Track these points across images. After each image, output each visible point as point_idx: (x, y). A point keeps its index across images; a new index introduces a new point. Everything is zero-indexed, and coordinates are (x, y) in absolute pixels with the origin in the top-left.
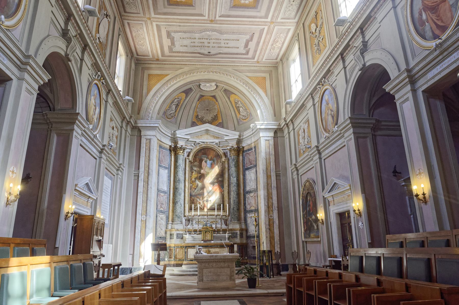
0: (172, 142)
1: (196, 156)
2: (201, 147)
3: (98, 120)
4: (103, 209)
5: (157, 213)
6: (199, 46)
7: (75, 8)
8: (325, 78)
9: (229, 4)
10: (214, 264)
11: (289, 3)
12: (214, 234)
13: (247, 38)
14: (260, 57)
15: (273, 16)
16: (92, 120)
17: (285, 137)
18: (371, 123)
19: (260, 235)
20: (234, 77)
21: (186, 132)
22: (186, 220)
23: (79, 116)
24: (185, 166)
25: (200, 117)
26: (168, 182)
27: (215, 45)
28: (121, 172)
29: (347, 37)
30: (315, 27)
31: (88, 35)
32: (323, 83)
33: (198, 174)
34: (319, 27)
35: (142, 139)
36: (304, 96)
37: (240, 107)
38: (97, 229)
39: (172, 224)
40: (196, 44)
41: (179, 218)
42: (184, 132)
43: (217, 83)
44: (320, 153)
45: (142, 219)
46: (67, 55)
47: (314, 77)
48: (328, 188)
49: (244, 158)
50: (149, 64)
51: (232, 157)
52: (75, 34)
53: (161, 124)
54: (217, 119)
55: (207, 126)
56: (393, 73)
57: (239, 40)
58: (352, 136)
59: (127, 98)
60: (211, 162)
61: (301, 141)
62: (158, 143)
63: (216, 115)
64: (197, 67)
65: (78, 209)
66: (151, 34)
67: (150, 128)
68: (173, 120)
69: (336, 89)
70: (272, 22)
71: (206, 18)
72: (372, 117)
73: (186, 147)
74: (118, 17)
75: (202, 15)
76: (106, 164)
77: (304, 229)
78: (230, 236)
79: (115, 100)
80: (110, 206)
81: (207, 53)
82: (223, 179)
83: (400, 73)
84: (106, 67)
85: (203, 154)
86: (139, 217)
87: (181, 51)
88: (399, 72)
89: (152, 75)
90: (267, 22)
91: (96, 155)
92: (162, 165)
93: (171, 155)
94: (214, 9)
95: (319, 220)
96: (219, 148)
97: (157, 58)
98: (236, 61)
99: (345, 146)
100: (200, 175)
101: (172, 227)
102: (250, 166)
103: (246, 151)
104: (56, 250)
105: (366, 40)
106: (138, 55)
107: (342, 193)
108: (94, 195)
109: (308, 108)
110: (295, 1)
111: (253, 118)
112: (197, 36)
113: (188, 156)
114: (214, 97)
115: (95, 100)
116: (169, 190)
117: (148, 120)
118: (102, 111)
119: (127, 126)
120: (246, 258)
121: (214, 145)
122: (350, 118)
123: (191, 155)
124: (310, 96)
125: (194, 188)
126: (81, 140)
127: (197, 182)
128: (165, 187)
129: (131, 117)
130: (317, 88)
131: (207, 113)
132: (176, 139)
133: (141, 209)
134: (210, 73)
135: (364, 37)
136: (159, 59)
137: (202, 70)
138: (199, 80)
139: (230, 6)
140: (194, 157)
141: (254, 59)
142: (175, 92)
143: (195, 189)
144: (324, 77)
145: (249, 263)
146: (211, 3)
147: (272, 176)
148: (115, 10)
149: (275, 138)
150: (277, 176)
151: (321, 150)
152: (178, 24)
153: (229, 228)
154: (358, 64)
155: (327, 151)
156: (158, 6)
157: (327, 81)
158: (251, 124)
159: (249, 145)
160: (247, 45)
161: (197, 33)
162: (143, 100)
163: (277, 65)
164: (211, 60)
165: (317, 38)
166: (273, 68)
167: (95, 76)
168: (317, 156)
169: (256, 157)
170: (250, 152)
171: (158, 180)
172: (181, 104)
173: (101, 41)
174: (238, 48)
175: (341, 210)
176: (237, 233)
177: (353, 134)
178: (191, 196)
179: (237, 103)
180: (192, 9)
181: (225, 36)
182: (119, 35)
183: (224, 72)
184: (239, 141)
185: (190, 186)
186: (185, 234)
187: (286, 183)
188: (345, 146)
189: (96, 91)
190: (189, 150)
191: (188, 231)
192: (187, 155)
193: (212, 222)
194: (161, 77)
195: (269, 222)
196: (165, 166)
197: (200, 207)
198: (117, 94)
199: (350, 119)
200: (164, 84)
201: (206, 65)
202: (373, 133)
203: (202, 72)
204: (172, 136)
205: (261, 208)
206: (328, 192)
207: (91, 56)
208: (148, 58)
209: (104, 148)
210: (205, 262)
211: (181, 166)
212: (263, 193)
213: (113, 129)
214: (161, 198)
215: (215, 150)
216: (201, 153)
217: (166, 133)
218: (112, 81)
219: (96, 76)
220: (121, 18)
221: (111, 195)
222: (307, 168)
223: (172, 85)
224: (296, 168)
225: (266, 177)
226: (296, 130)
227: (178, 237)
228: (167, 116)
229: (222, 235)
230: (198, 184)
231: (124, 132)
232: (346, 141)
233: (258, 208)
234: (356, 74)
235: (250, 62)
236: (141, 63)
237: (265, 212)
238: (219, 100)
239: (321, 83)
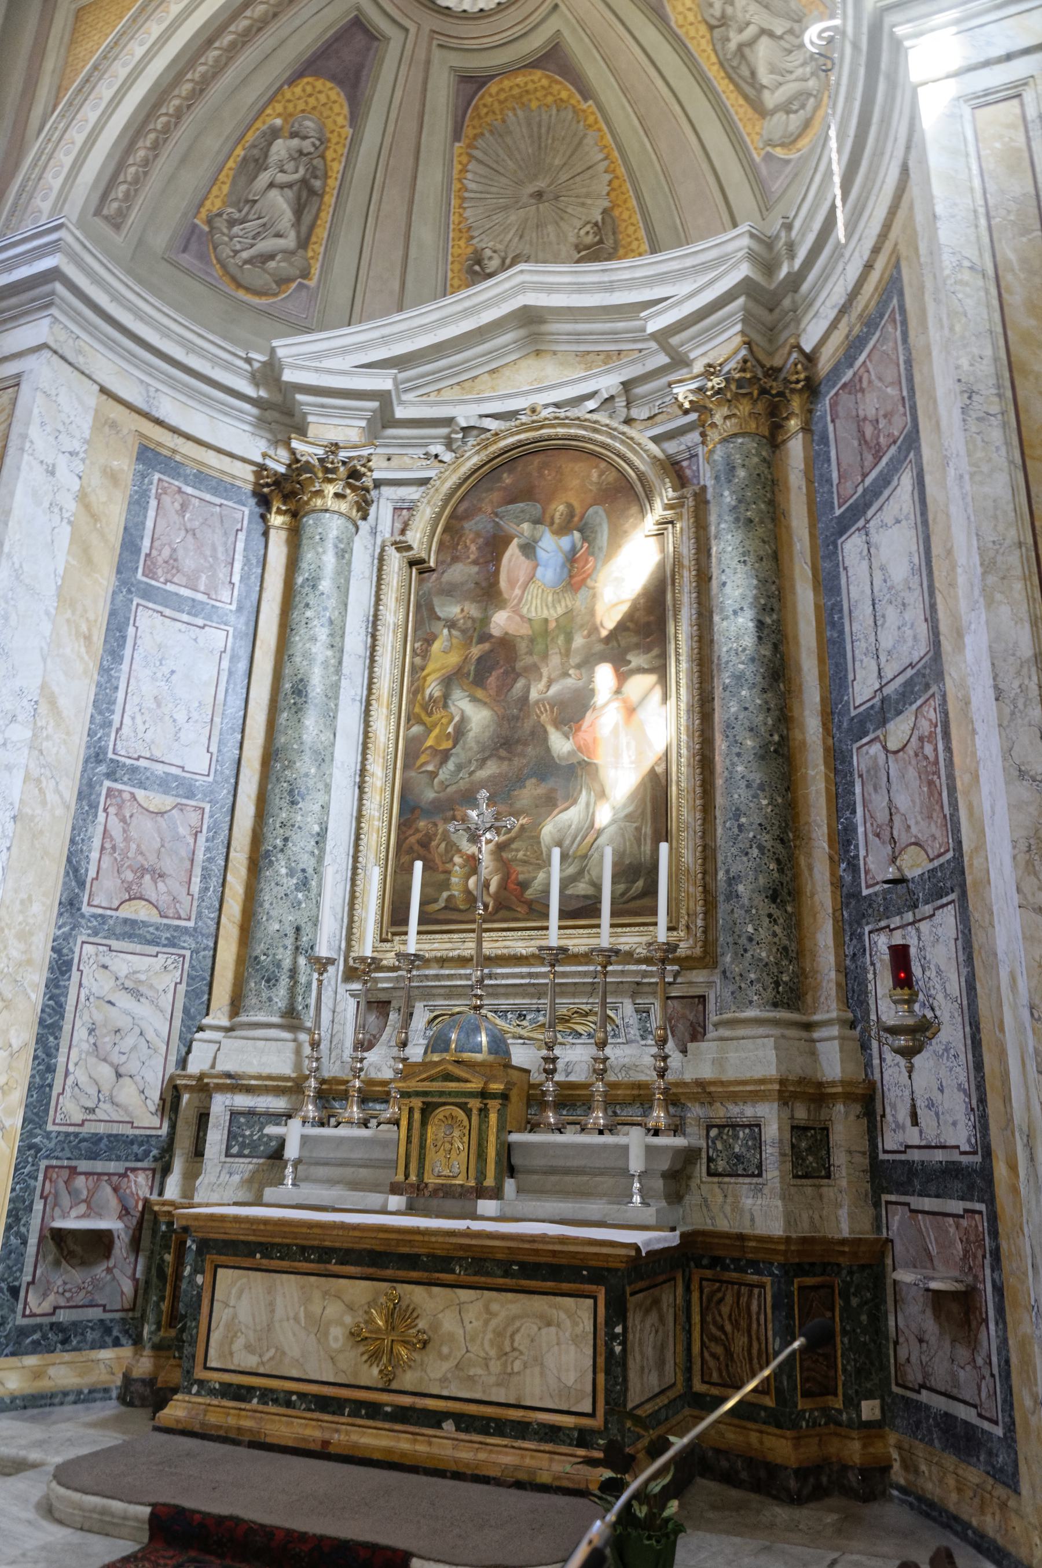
2: (493, 449)
12: (533, 1127)
19: (1000, 1170)
33: (468, 643)
42: (345, 351)
55: (522, 288)
60: (565, 542)
63: (605, 212)
78: (689, 1156)
85: (512, 501)
96: (625, 428)
100: (486, 646)
120: (870, 1409)
125: (434, 751)
127: (462, 704)
131: (540, 226)
140: (445, 530)
143: (445, 756)
172: (333, 183)
176: (755, 1126)
204: (263, 393)
205: (980, 846)
216: (496, 496)
228: (233, 270)
230: (464, 720)
233: (959, 843)
238: (594, 71)
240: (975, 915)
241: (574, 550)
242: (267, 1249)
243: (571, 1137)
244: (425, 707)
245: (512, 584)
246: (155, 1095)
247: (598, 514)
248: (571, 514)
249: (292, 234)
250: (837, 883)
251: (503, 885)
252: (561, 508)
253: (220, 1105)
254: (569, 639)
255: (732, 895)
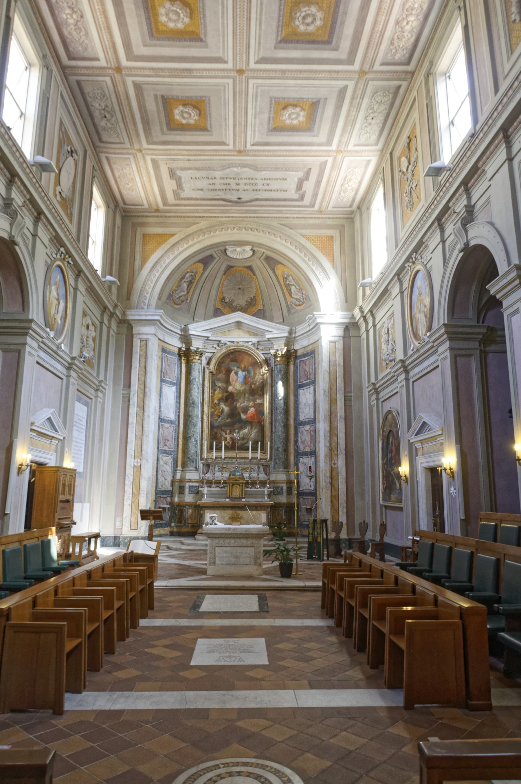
0: (182, 342)
1: (220, 363)
3: (63, 320)
4: (75, 451)
5: (158, 454)
6: (223, 190)
7: (21, 165)
8: (416, 253)
9: (266, 127)
10: (232, 541)
11: (365, 121)
12: (247, 487)
13: (299, 176)
14: (323, 204)
15: (340, 141)
16: (55, 322)
17: (362, 337)
18: (478, 334)
19: (318, 492)
20: (280, 237)
21: (205, 326)
22: (203, 465)
23: (33, 324)
24: (204, 380)
25: (227, 300)
26: (176, 406)
27: (246, 187)
28: (102, 392)
29: (446, 195)
30: (406, 164)
31: (42, 198)
32: (414, 260)
33: (223, 392)
34: (412, 163)
35: (134, 339)
36: (388, 276)
37: (292, 285)
38: (64, 485)
39: (182, 471)
40: (217, 187)
41: (193, 462)
42: (201, 326)
43: (253, 246)
44: (407, 371)
45: (136, 464)
46: (11, 237)
47: (403, 245)
48: (416, 426)
49: (297, 368)
50: (143, 216)
51: (278, 366)
52: (23, 201)
53: (163, 316)
54: (255, 304)
55: (238, 316)
56: (502, 267)
57: (286, 179)
58: (448, 353)
59: (109, 278)
60: (244, 373)
61: (384, 347)
62: (159, 345)
63: (254, 296)
64: (220, 222)
65: (36, 456)
66: (144, 174)
67: (146, 322)
68: (184, 306)
69: (431, 273)
70: (338, 151)
71: (231, 147)
72: (483, 322)
73: (205, 350)
74: (90, 149)
75: (223, 144)
76: (78, 384)
77: (383, 486)
78: (271, 492)
79: (89, 285)
80: (85, 445)
81: (236, 200)
82: (263, 401)
83: (510, 268)
84: (72, 240)
86: (130, 461)
87: (194, 197)
88: (509, 267)
89: (149, 235)
90: (330, 151)
91: (63, 374)
92: (167, 379)
93: (181, 364)
94: (243, 134)
95: (401, 477)
96: (257, 351)
97: (156, 208)
98: (283, 210)
99: (438, 366)
100: (227, 394)
101: (181, 475)
102: (306, 382)
103: (301, 357)
104: (6, 517)
105: (473, 203)
106: (125, 204)
107: (433, 438)
108: (60, 434)
109: (393, 296)
110: (375, 118)
111: (311, 305)
112: (218, 174)
113: (208, 364)
114: (250, 268)
115: (57, 290)
116: (177, 418)
117: (144, 309)
118: (68, 306)
119: (109, 321)
121: (250, 346)
122: (444, 325)
123: (213, 362)
124: (396, 278)
125: (217, 415)
126: (38, 356)
127: (223, 406)
128: (170, 414)
129: (116, 306)
130: (405, 267)
132: (188, 338)
133: (134, 449)
134: (242, 230)
135: (469, 198)
136: (160, 209)
137: (229, 226)
138: (225, 242)
139: (269, 129)
140: (218, 365)
141: (313, 206)
142: (185, 262)
143: (219, 416)
144: (416, 250)
145: (299, 533)
146: (237, 125)
147: (338, 399)
148: (85, 140)
149: (346, 339)
150: (347, 399)
151: (409, 367)
152: (186, 157)
153: (271, 479)
154: (459, 242)
155: (416, 370)
156: (152, 131)
157: (419, 257)
158: (307, 315)
159: (305, 347)
160: (300, 186)
161: (218, 170)
162: (135, 277)
163: (352, 216)
164: (243, 210)
165: (408, 183)
166: (345, 220)
167: (56, 254)
168: (403, 376)
169: (315, 368)
170: (306, 358)
171: (160, 403)
172: (196, 280)
173: (64, 196)
174: (286, 191)
175: (431, 465)
176: (282, 487)
177: (448, 351)
178: (212, 427)
179: (286, 278)
180: (206, 135)
181: (264, 174)
182: (93, 177)
183: (264, 229)
184: (289, 341)
185: (211, 412)
186: (202, 487)
187: (360, 411)
188: (438, 366)
189: (59, 277)
190: (210, 355)
191: (207, 483)
192: (206, 362)
193: (245, 469)
194: (163, 238)
195: (331, 473)
196: (171, 380)
197: (225, 445)
198: (92, 275)
199: (445, 327)
200: (168, 250)
201: (236, 217)
202: (482, 348)
203: (229, 230)
206: (414, 435)
207: (49, 227)
208: (142, 209)
209: (73, 361)
210: (218, 537)
211: (197, 380)
212: (323, 427)
213: (88, 327)
214: (166, 430)
215: (250, 355)
216: (229, 360)
217: (172, 329)
218: (83, 257)
219: (58, 254)
220: (95, 150)
221: (86, 428)
222: (390, 392)
223: (181, 252)
224: (376, 389)
225: (328, 402)
226: (378, 326)
227: (190, 492)
229: (259, 489)
230: (223, 409)
231: (105, 329)
232: (440, 358)
233: (316, 449)
234: (456, 257)
235: (307, 212)
236: (132, 216)
237: (326, 456)
238: (257, 272)
239: (411, 260)
240: (318, 460)
241: (246, 375)
242: (214, 507)
243: (253, 489)
244: (214, 405)
245: (233, 381)
246: (170, 483)
247: (251, 368)
248: (245, 367)
249: (186, 292)
250: (295, 449)
251: (232, 443)
252: (243, 365)
253: (187, 485)
254: (245, 395)
255: (278, 450)
